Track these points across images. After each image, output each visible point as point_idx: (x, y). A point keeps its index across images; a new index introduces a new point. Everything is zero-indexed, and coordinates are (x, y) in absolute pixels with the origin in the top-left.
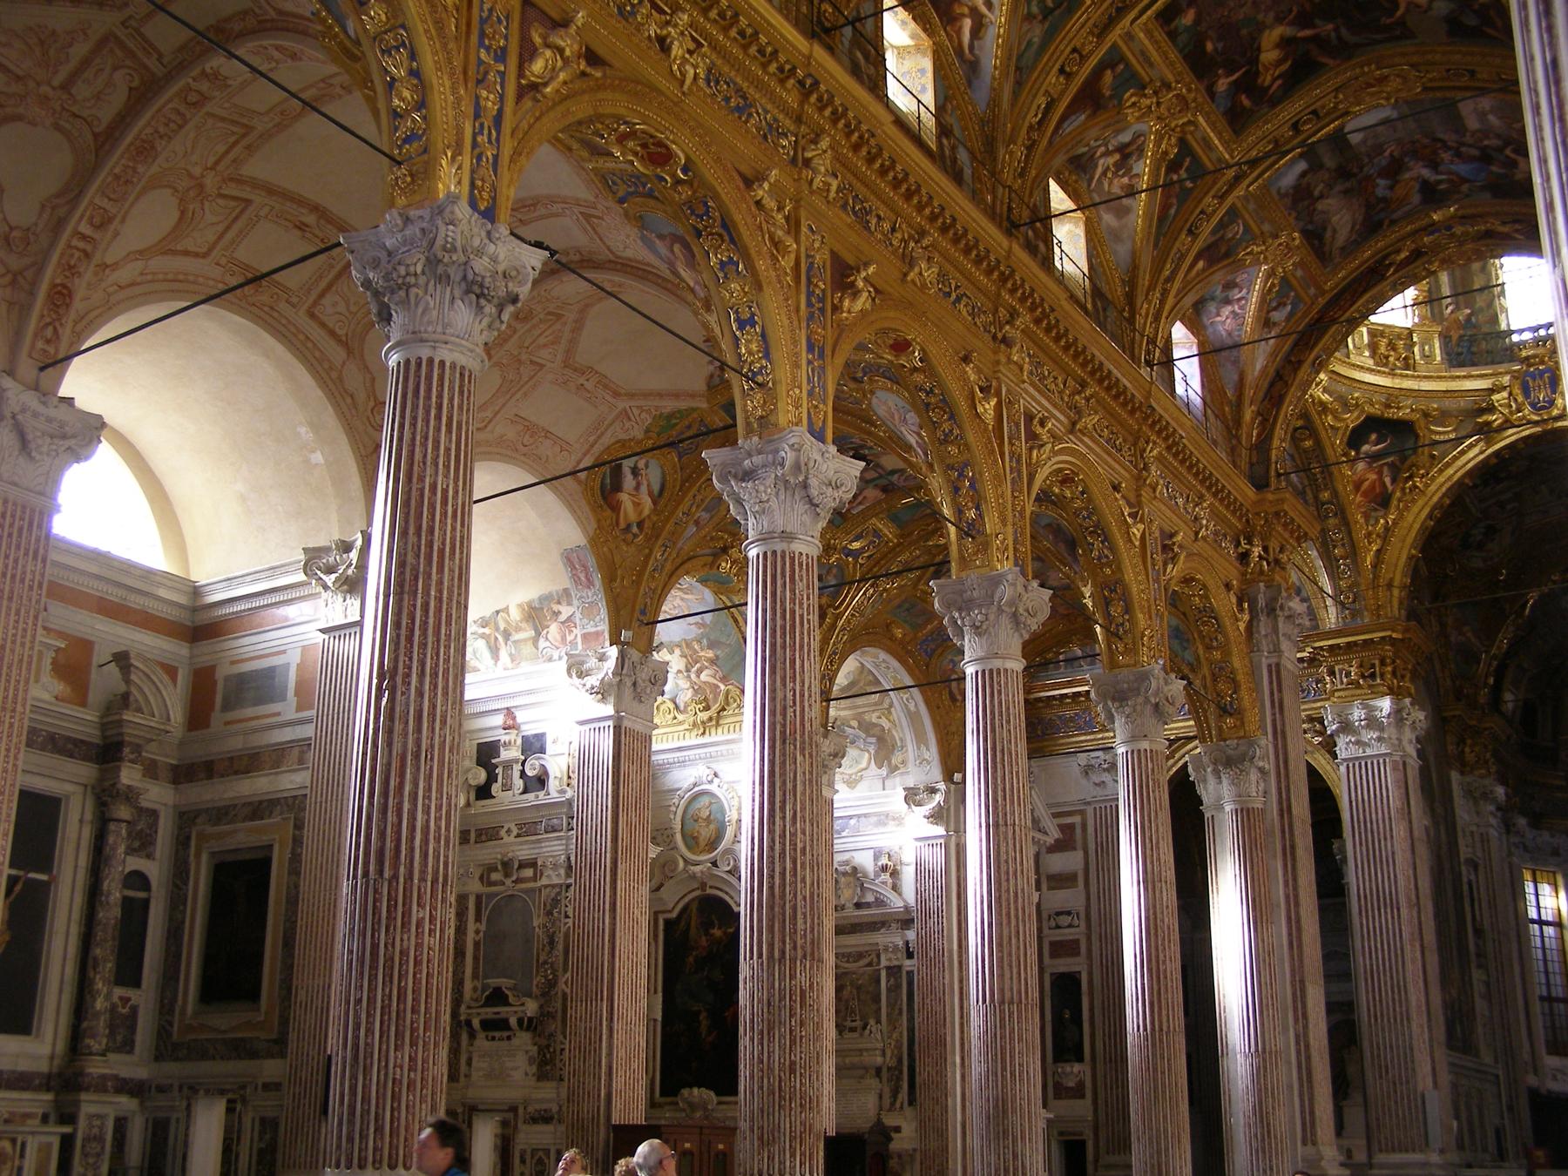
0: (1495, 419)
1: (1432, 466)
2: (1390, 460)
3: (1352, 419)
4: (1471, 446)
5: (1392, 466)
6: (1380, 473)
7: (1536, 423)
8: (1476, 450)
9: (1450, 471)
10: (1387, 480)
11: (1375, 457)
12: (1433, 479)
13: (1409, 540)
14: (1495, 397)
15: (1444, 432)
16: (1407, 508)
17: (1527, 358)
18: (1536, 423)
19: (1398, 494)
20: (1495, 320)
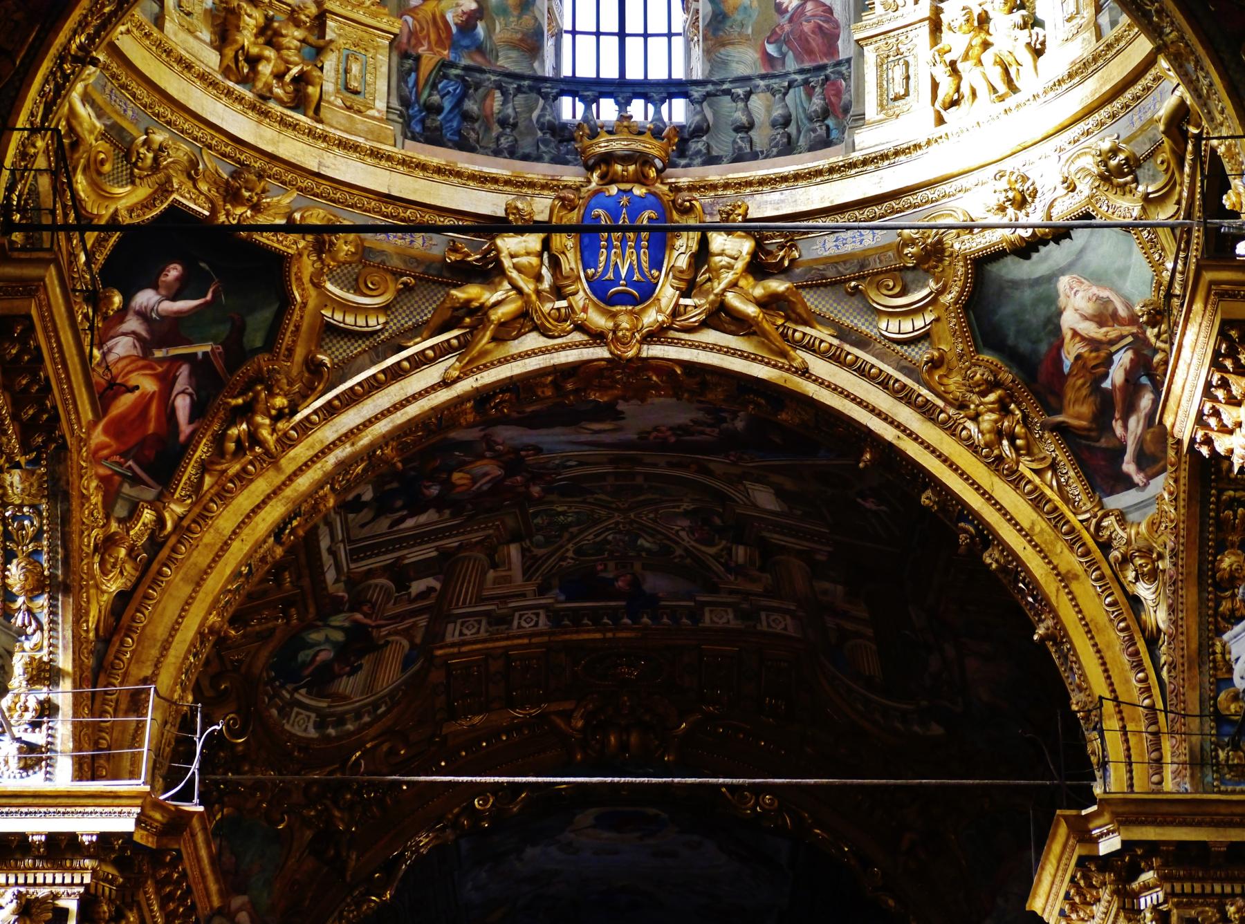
0: (498, 300)
1: (307, 393)
2: (201, 349)
3: (127, 199)
4: (420, 361)
5: (199, 366)
6: (167, 382)
7: (597, 337)
8: (432, 375)
9: (350, 419)
10: (182, 405)
11: (163, 331)
12: (305, 427)
13: (214, 583)
14: (508, 244)
15: (365, 308)
16: (223, 496)
17: (608, 158)
18: (597, 337)
19: (202, 451)
20: (531, 44)
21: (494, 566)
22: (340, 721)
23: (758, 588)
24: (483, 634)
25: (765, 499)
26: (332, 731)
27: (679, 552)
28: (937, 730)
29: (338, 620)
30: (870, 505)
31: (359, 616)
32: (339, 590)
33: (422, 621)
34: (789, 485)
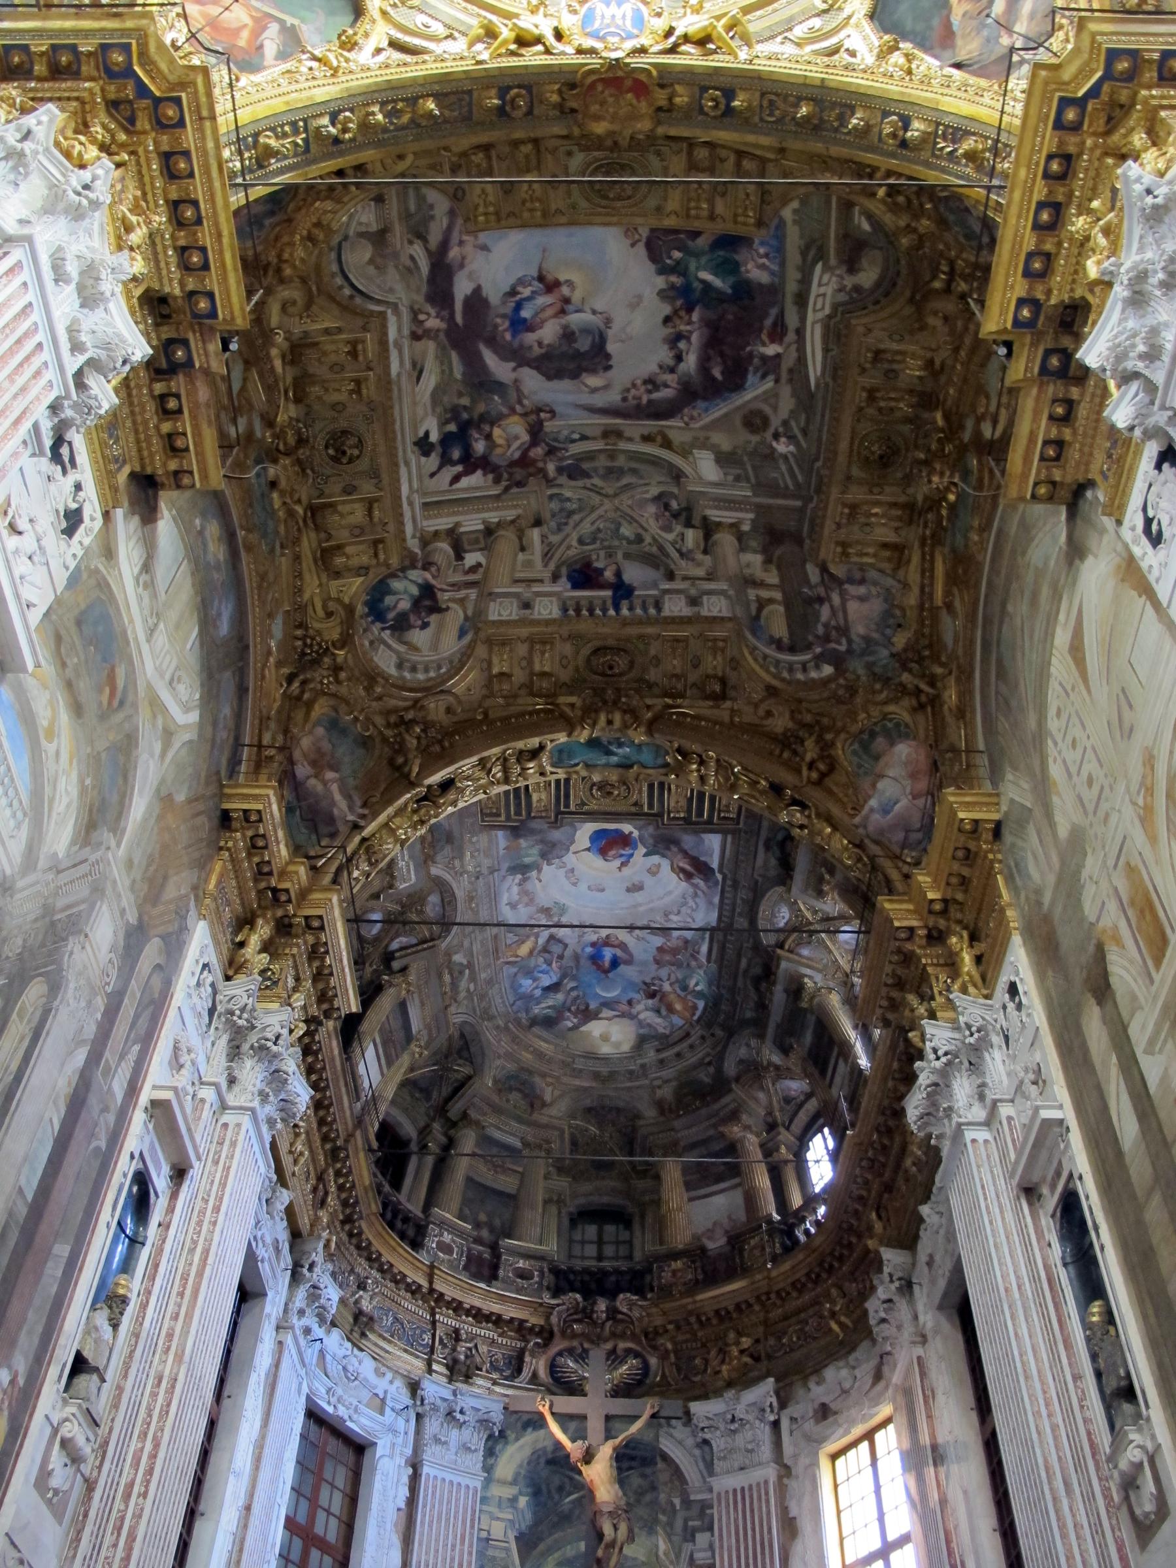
2: (290, 21)
18: (592, 51)
21: (523, 549)
22: (414, 669)
23: (700, 572)
24: (514, 617)
25: (706, 468)
26: (407, 675)
27: (648, 540)
28: (828, 670)
29: (414, 574)
30: (782, 447)
31: (428, 576)
32: (413, 545)
33: (473, 594)
34: (725, 443)
